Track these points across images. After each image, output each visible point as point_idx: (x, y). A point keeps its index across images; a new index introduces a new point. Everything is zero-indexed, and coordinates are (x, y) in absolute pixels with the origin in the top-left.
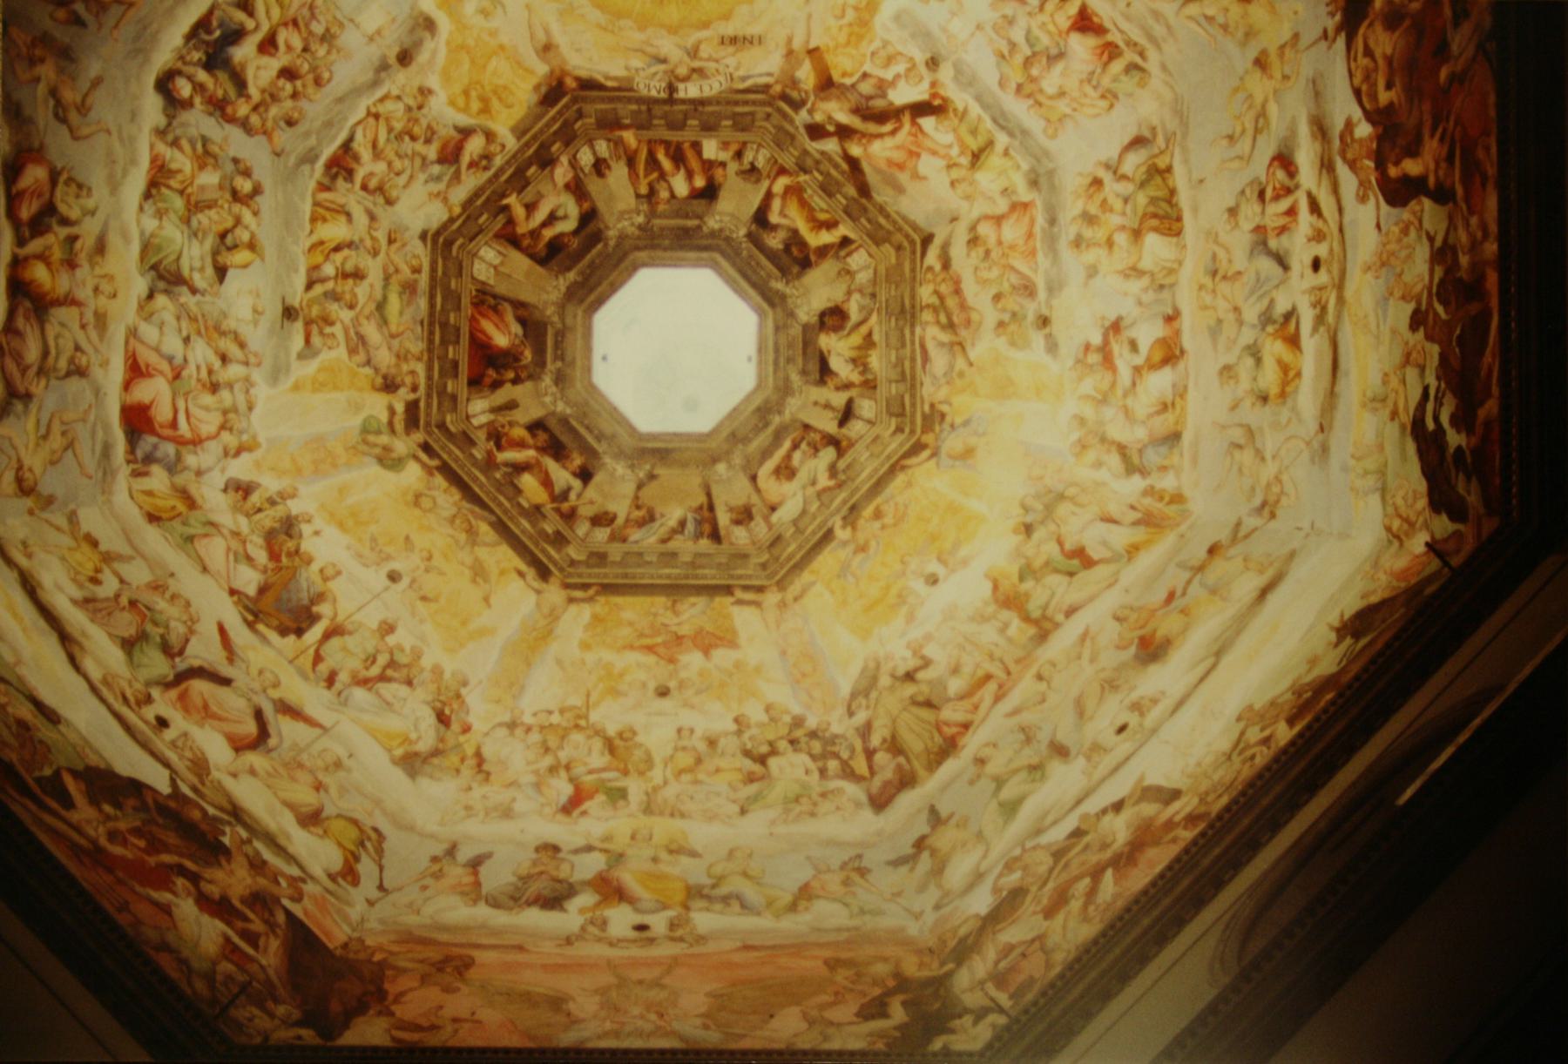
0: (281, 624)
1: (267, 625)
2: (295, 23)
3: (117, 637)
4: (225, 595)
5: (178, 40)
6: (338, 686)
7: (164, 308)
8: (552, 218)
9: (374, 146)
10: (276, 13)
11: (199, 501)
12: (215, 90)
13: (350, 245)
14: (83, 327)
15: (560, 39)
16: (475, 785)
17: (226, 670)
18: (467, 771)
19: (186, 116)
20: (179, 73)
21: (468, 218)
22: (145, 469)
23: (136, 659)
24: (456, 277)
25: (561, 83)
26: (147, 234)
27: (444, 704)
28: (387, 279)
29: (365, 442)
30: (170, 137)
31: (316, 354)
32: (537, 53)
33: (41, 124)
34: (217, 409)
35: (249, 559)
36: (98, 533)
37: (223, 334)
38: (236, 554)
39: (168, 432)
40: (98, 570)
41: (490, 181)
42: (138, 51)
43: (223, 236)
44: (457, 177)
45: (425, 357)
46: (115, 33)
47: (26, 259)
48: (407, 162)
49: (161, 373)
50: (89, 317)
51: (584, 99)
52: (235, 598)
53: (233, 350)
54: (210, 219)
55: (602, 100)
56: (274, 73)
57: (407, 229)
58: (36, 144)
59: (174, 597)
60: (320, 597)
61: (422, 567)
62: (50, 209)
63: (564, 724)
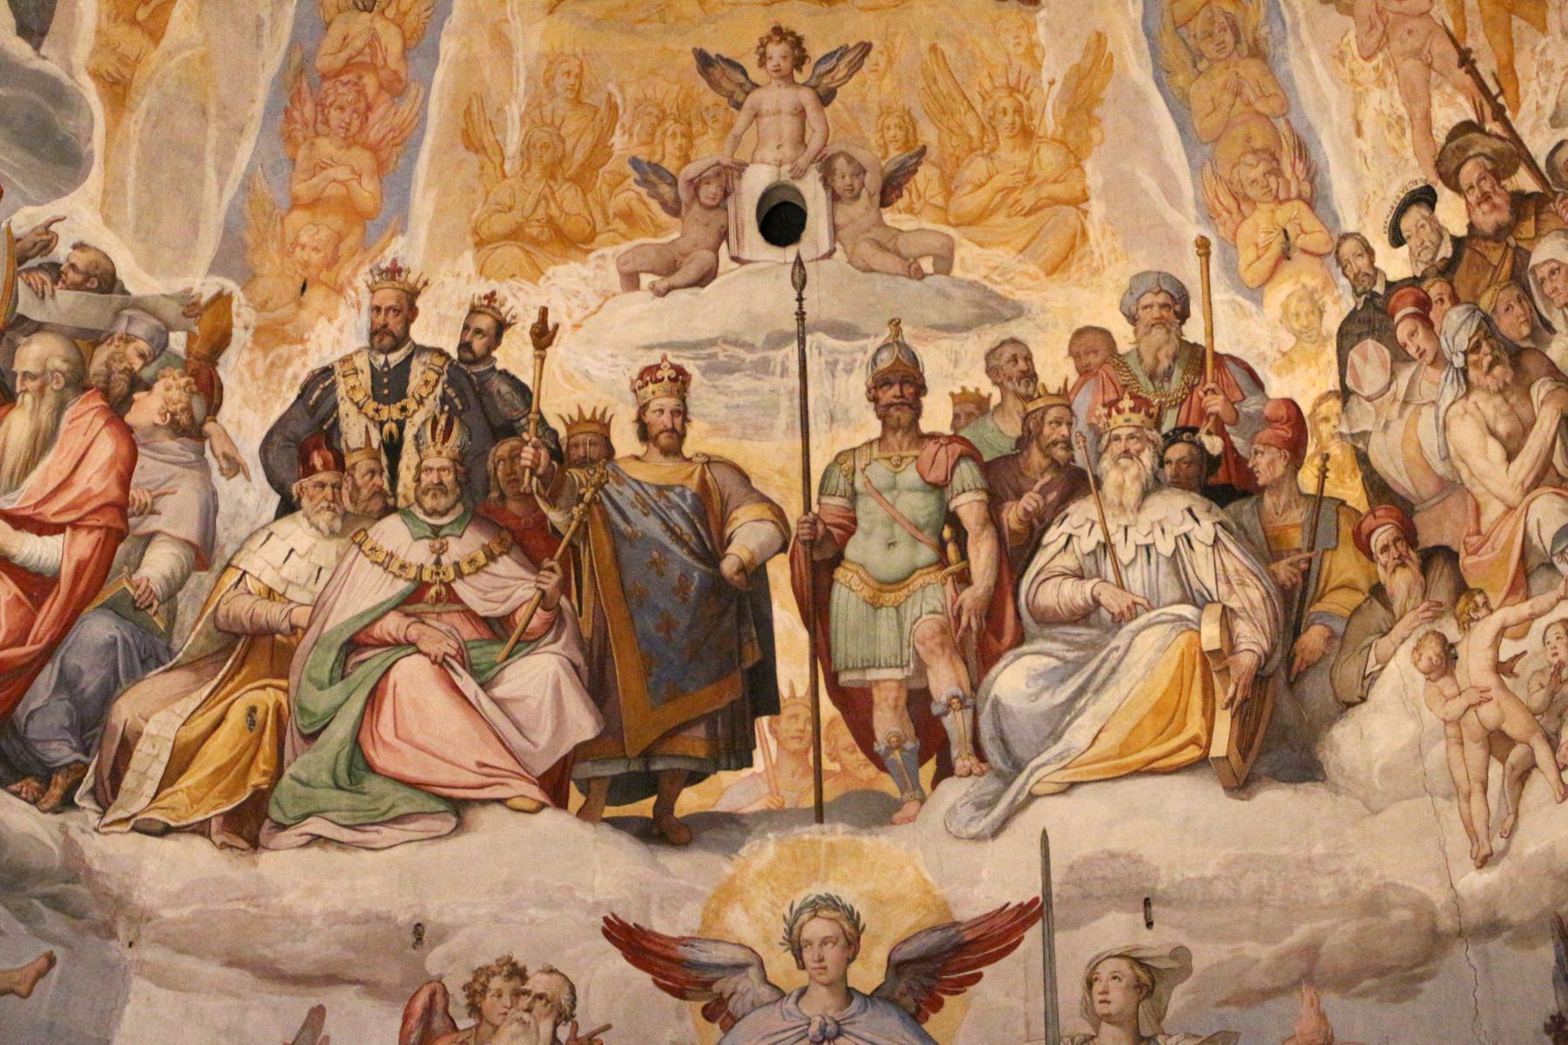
0: (710, 719)
1: (695, 778)
4: (550, 817)
6: (956, 725)
11: (271, 613)
16: (1450, 630)
18: (1401, 583)
22: (112, 747)
27: (1184, 432)
52: (576, 798)
59: (475, 994)
61: (807, 97)
63: (1488, 220)
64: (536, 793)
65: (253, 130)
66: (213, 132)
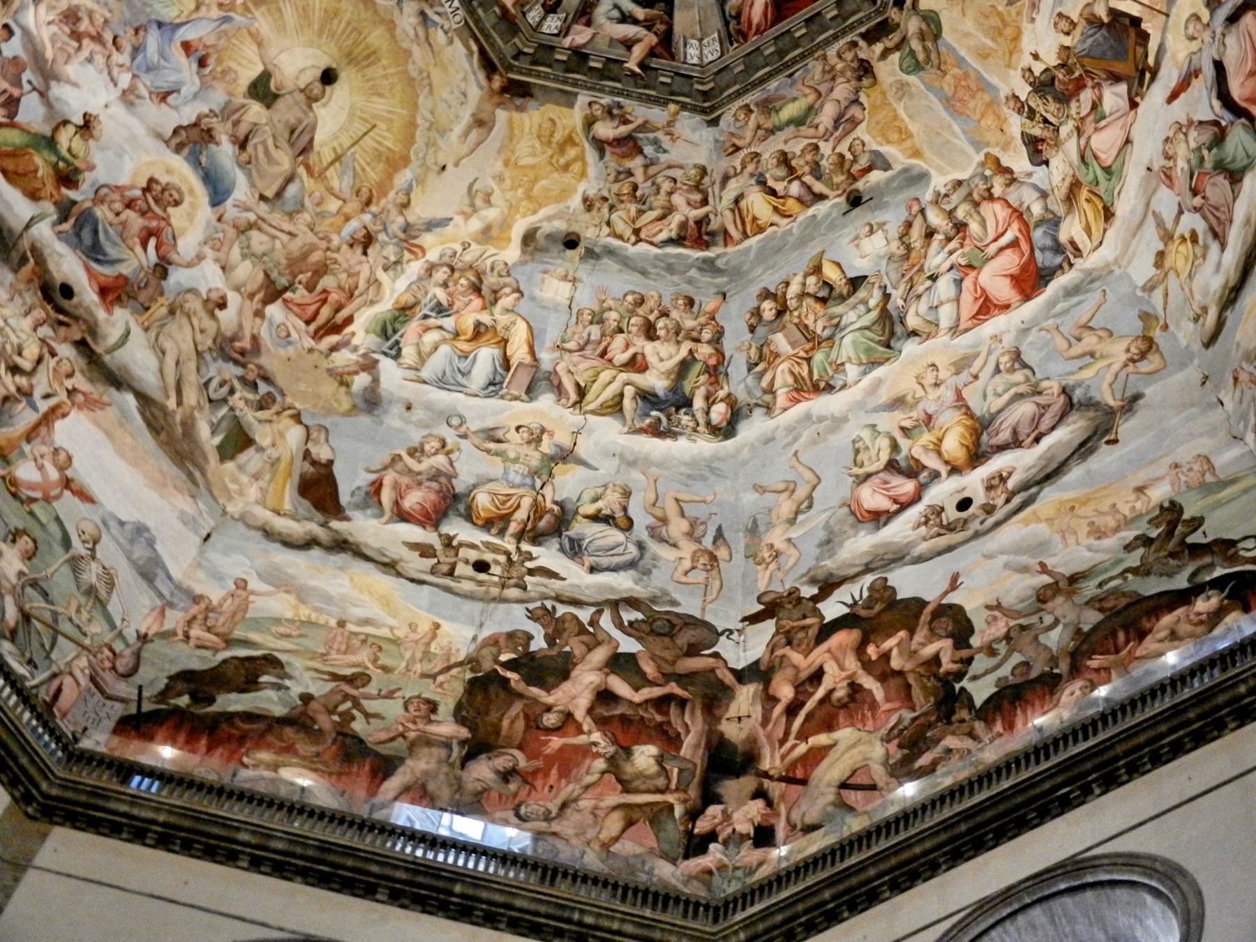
0: (1137, 43)
1: (1147, 56)
2: (603, 354)
3: (1233, 191)
4: (1140, 110)
5: (682, 442)
7: (917, 314)
8: (625, 18)
9: (662, 218)
10: (605, 376)
11: (1068, 180)
12: (703, 384)
13: (762, 183)
14: (976, 377)
15: (466, 118)
17: (1209, 71)
19: (742, 396)
20: (708, 423)
21: (672, 94)
22: (1069, 247)
23: (1245, 162)
24: (732, 70)
25: (504, 90)
26: (862, 368)
28: (771, 132)
29: (928, 58)
30: (768, 398)
31: (877, 154)
32: (491, 129)
33: (824, 516)
34: (979, 213)
35: (1095, 106)
36: (1152, 260)
37: (909, 248)
38: (1097, 122)
39: (1024, 246)
40: (1183, 239)
41: (628, 96)
42: (712, 470)
43: (823, 301)
44: (644, 127)
45: (820, 53)
46: (709, 498)
47: (947, 463)
48: (659, 179)
49: (975, 284)
50: (965, 376)
51: (502, 59)
52: (1138, 99)
53: (917, 232)
54: (816, 321)
55: (493, 45)
56: (657, 343)
57: (717, 141)
58: (846, 510)
59: (1168, 158)
60: (1094, 21)
62: (892, 466)
64: (1133, 112)
65: (953, 122)
66: (945, 134)
